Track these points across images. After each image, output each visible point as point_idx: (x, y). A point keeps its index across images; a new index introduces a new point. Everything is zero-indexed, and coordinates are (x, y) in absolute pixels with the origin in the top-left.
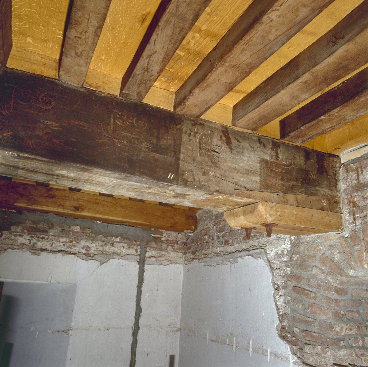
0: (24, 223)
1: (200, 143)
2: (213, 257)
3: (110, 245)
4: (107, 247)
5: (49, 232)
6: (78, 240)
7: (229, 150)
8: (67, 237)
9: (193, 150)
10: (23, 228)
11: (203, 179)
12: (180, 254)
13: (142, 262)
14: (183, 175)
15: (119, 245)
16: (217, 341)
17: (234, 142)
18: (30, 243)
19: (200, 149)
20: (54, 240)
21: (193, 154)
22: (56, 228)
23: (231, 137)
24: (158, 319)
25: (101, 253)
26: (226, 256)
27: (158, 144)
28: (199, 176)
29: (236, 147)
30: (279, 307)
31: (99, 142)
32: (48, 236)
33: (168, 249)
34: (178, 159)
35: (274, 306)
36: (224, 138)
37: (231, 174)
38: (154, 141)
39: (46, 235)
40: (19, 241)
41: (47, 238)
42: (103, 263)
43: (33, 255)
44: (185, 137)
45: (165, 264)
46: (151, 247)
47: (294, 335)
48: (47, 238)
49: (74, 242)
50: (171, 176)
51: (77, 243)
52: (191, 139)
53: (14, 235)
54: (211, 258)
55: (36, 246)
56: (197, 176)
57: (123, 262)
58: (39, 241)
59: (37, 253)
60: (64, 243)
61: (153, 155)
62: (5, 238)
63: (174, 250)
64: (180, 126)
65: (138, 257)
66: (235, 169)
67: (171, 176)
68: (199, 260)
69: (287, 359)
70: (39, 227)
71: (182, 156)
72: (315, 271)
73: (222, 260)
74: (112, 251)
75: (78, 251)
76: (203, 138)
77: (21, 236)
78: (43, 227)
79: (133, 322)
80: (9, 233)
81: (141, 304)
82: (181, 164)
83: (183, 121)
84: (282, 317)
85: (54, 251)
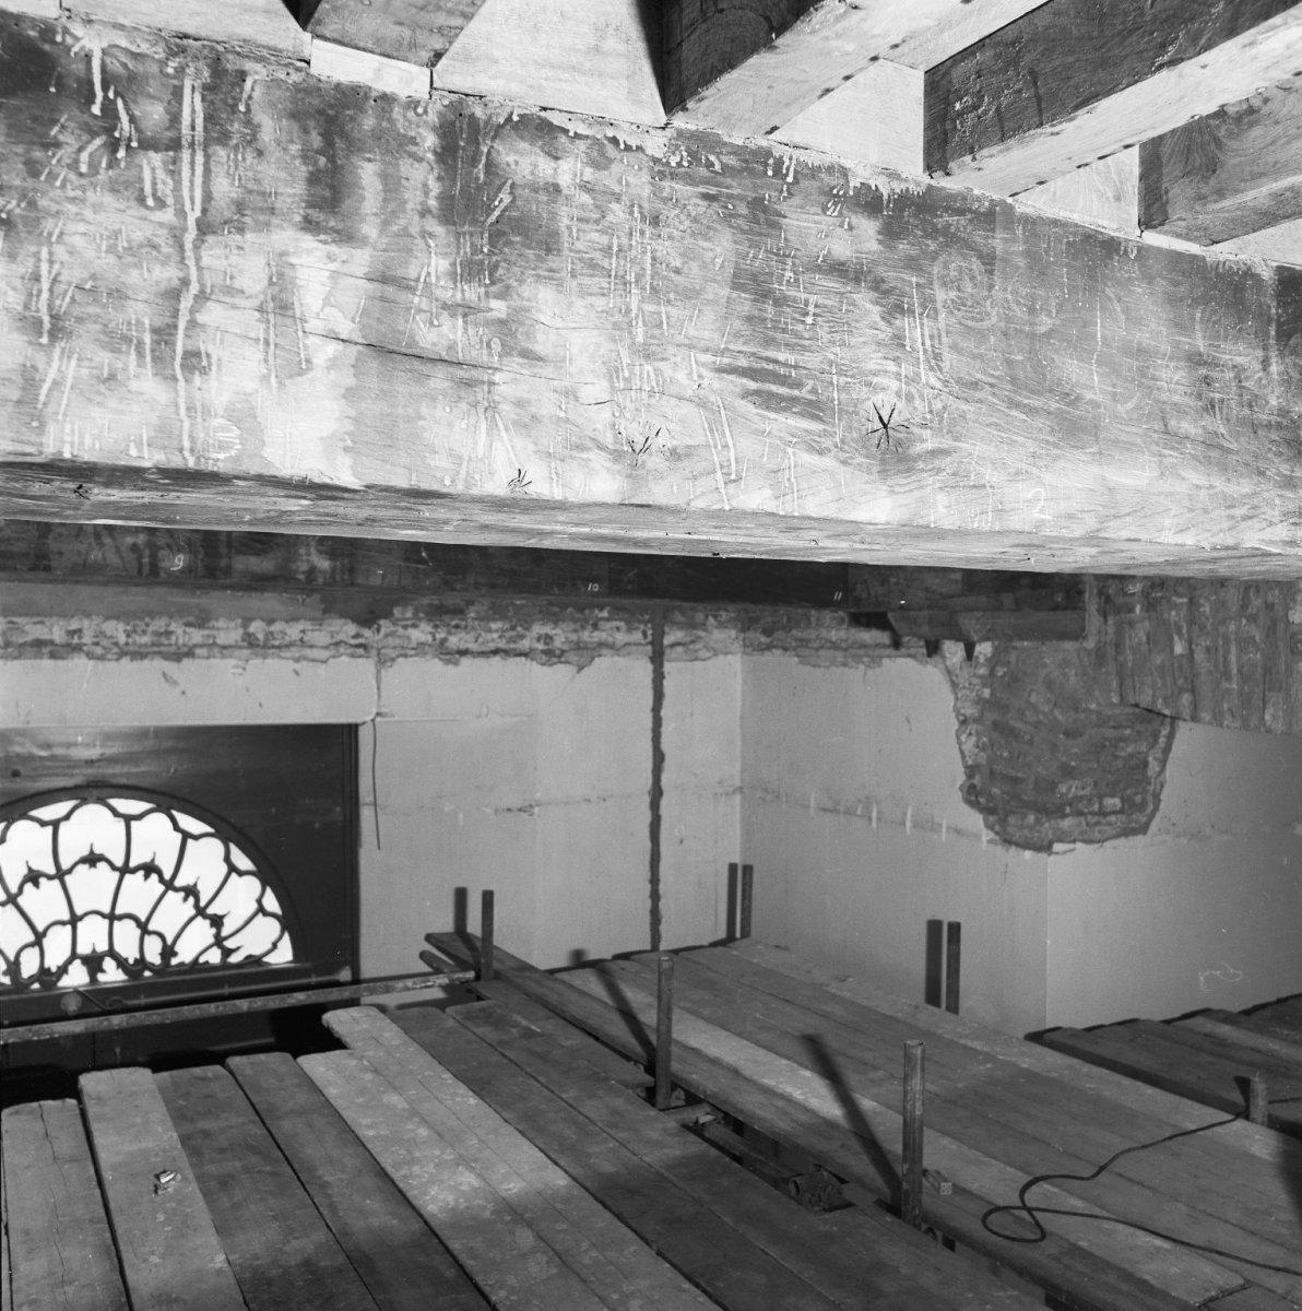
2: (822, 647)
4: (586, 633)
8: (504, 618)
12: (733, 633)
13: (657, 659)
15: (609, 625)
16: (835, 811)
26: (853, 651)
30: (966, 752)
35: (957, 751)
40: (413, 637)
41: (466, 627)
46: (674, 623)
47: (991, 798)
48: (466, 627)
49: (519, 629)
51: (526, 629)
54: (817, 649)
55: (447, 644)
57: (620, 661)
58: (450, 633)
62: (386, 636)
63: (721, 625)
65: (649, 648)
68: (785, 649)
69: (977, 836)
72: (1033, 699)
73: (845, 657)
74: (596, 640)
77: (415, 626)
79: (650, 782)
84: (971, 771)
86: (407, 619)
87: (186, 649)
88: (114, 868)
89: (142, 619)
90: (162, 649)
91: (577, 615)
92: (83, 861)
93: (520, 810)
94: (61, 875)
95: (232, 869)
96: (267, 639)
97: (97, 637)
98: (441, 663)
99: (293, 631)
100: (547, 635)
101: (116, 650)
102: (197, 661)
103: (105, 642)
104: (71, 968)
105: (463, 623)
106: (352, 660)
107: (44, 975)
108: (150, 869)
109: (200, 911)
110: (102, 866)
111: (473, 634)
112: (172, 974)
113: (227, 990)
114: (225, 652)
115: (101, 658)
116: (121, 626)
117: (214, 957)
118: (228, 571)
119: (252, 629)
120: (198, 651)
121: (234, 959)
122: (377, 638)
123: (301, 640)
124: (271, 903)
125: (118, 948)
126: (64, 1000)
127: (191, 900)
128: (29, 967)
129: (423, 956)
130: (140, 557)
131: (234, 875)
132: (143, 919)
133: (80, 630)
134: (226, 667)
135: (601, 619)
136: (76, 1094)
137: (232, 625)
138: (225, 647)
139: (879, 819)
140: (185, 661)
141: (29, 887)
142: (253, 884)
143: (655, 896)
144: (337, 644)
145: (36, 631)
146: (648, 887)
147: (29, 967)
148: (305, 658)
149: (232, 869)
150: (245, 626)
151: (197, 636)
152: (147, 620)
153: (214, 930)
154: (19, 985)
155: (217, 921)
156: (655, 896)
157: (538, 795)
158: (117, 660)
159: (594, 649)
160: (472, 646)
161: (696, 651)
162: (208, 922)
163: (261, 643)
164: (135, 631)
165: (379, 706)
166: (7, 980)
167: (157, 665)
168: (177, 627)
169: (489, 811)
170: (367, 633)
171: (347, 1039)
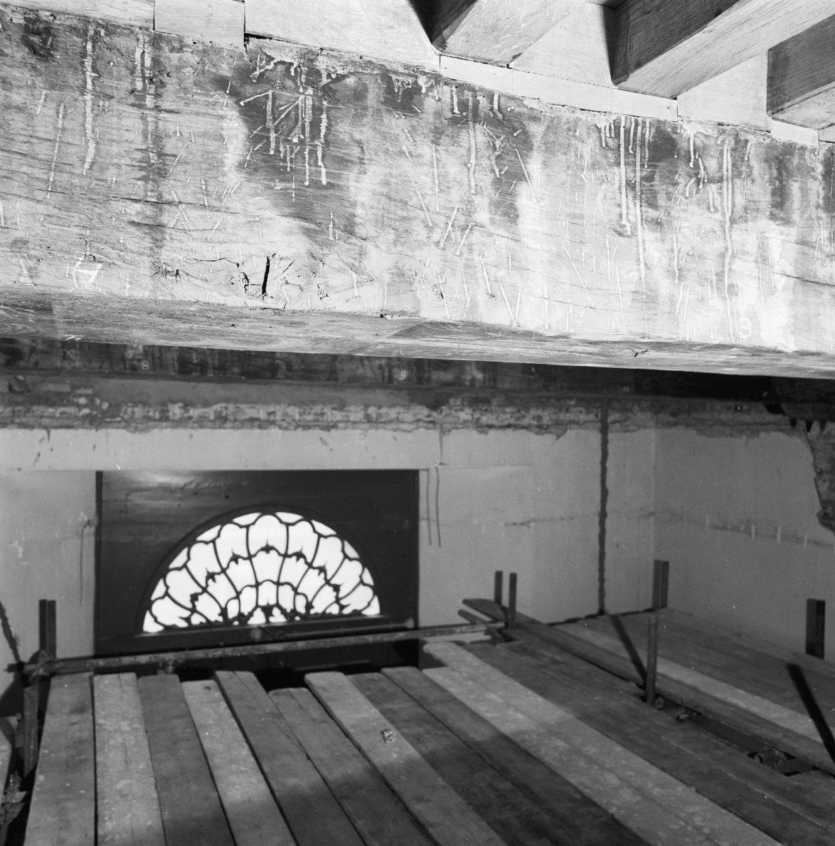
12: (649, 415)
13: (604, 431)
15: (575, 409)
16: (724, 528)
18: (473, 418)
30: (822, 493)
49: (523, 412)
54: (710, 426)
55: (481, 421)
57: (582, 432)
58: (482, 415)
62: (446, 416)
63: (642, 410)
74: (568, 419)
77: (462, 410)
87: (332, 424)
88: (280, 554)
89: (308, 405)
90: (320, 423)
92: (263, 549)
93: (522, 524)
94: (250, 557)
95: (346, 556)
96: (377, 418)
99: (393, 413)
101: (294, 424)
103: (288, 419)
105: (489, 408)
107: (242, 618)
108: (299, 555)
109: (328, 582)
110: (273, 553)
113: (342, 630)
114: (355, 425)
115: (286, 429)
116: (297, 410)
117: (335, 610)
118: (429, 380)
120: (340, 425)
121: (346, 611)
122: (440, 417)
123: (397, 418)
124: (368, 578)
125: (281, 603)
126: (253, 632)
128: (232, 613)
129: (462, 613)
130: (383, 372)
131: (347, 561)
134: (356, 433)
135: (572, 406)
136: (306, 685)
137: (358, 409)
138: (354, 422)
139: (757, 534)
140: (333, 431)
141: (233, 564)
142: (357, 566)
143: (602, 580)
144: (418, 421)
145: (250, 412)
147: (232, 613)
148: (399, 429)
149: (346, 556)
151: (338, 416)
152: (311, 406)
155: (336, 588)
156: (602, 580)
158: (295, 429)
160: (494, 422)
161: (628, 426)
166: (220, 619)
167: (317, 433)
168: (327, 410)
169: (502, 524)
170: (435, 414)
171: (444, 660)
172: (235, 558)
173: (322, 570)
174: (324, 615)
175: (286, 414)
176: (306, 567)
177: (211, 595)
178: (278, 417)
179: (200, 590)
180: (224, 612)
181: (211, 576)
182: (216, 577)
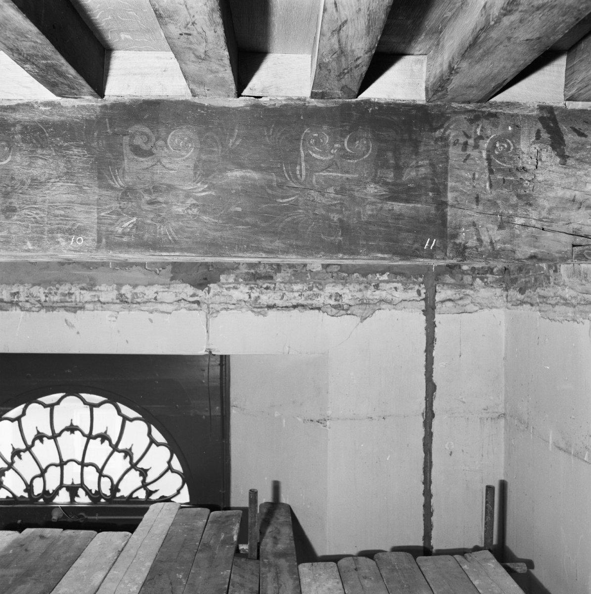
0: (237, 268)
1: (489, 159)
2: (557, 304)
3: (372, 287)
4: (369, 292)
5: (274, 278)
6: (321, 285)
7: (558, 160)
8: (303, 281)
9: (474, 178)
10: (236, 276)
11: (499, 238)
12: (499, 291)
13: (430, 311)
14: (455, 236)
17: (570, 138)
18: (250, 297)
19: (491, 172)
20: (284, 289)
21: (474, 187)
22: (284, 270)
23: (564, 128)
24: (464, 400)
25: (360, 302)
26: (581, 308)
27: (398, 181)
28: (491, 232)
29: (576, 150)
31: (284, 203)
32: (275, 284)
33: (475, 284)
34: (442, 205)
36: (545, 136)
37: (564, 215)
38: (390, 176)
39: (273, 283)
40: (234, 296)
41: (274, 288)
42: (366, 319)
43: (258, 316)
44: (454, 152)
45: (472, 311)
46: (444, 284)
48: (274, 288)
49: (315, 289)
50: (431, 243)
51: (320, 290)
52: (469, 156)
53: (226, 289)
54: (553, 305)
55: (259, 301)
56: (486, 233)
58: (262, 293)
59: (262, 313)
60: (300, 293)
61: (390, 208)
62: (215, 295)
63: (487, 285)
64: (442, 130)
65: (423, 303)
66: (574, 201)
67: (431, 243)
68: (532, 305)
70: (258, 271)
71: (450, 197)
74: (378, 297)
75: (324, 303)
76: (495, 147)
78: (264, 271)
80: (219, 285)
81: (433, 378)
82: (449, 214)
83: (448, 118)
85: (287, 307)
86: (230, 283)
88: (84, 435)
89: (54, 285)
90: (66, 304)
91: (361, 279)
92: (67, 429)
94: (54, 437)
95: (152, 441)
97: (28, 297)
98: (253, 314)
99: (150, 292)
100: (337, 293)
101: (39, 305)
102: (87, 312)
104: (60, 492)
106: (188, 312)
107: (49, 496)
108: (104, 437)
109: (133, 466)
110: (77, 433)
111: (279, 293)
112: (116, 503)
114: (104, 306)
116: (42, 290)
119: (123, 292)
120: (87, 306)
122: (208, 296)
123: (155, 299)
124: (176, 464)
127: (128, 458)
128: (38, 489)
131: (153, 445)
132: (100, 467)
133: (18, 293)
134: (106, 315)
135: (384, 281)
140: (79, 312)
141: (37, 442)
142: (165, 452)
143: (427, 494)
146: (422, 487)
147: (38, 489)
149: (152, 441)
150: (118, 289)
151: (87, 296)
152: (57, 286)
153: (141, 478)
154: (33, 499)
155: (144, 473)
156: (427, 494)
157: (329, 412)
158: (38, 312)
159: (375, 304)
162: (138, 473)
163: (129, 301)
164: (50, 293)
165: (208, 344)
166: (26, 495)
167: (62, 314)
168: (75, 290)
170: (200, 293)
172: (40, 437)
173: (128, 453)
174: (130, 499)
175: (31, 295)
176: (111, 449)
177: (16, 471)
178: (22, 298)
179: (6, 466)
180: (29, 488)
181: (16, 453)
182: (22, 453)
